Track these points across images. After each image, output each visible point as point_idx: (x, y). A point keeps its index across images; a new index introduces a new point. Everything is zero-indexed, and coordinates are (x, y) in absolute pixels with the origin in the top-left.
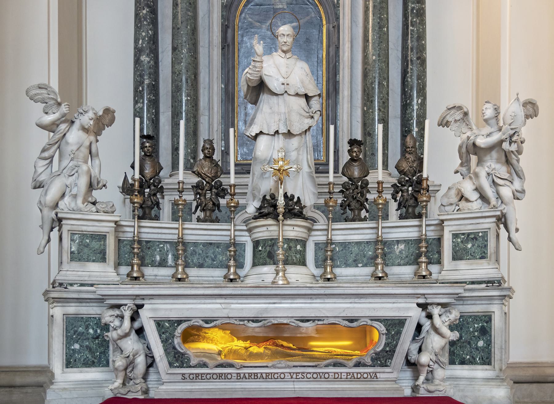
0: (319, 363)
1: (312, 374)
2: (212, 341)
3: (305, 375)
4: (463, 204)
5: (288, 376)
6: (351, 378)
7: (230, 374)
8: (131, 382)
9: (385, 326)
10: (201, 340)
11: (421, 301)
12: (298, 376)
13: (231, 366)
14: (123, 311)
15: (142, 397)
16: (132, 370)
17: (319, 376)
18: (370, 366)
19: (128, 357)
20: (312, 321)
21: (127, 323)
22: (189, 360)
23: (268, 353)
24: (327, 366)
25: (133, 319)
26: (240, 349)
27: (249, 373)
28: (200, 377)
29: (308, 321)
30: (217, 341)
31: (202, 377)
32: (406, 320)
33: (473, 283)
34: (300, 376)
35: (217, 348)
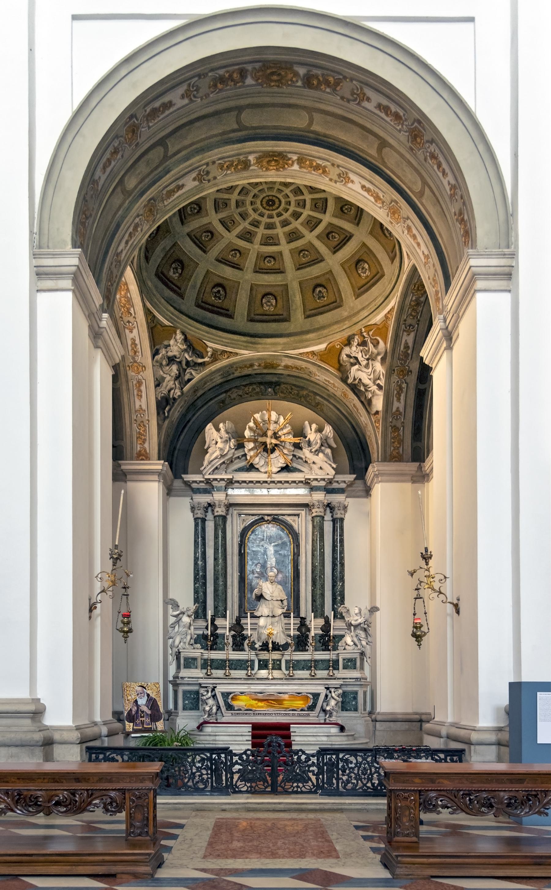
4: (347, 647)
11: (327, 686)
13: (251, 710)
21: (210, 694)
25: (212, 692)
33: (350, 679)
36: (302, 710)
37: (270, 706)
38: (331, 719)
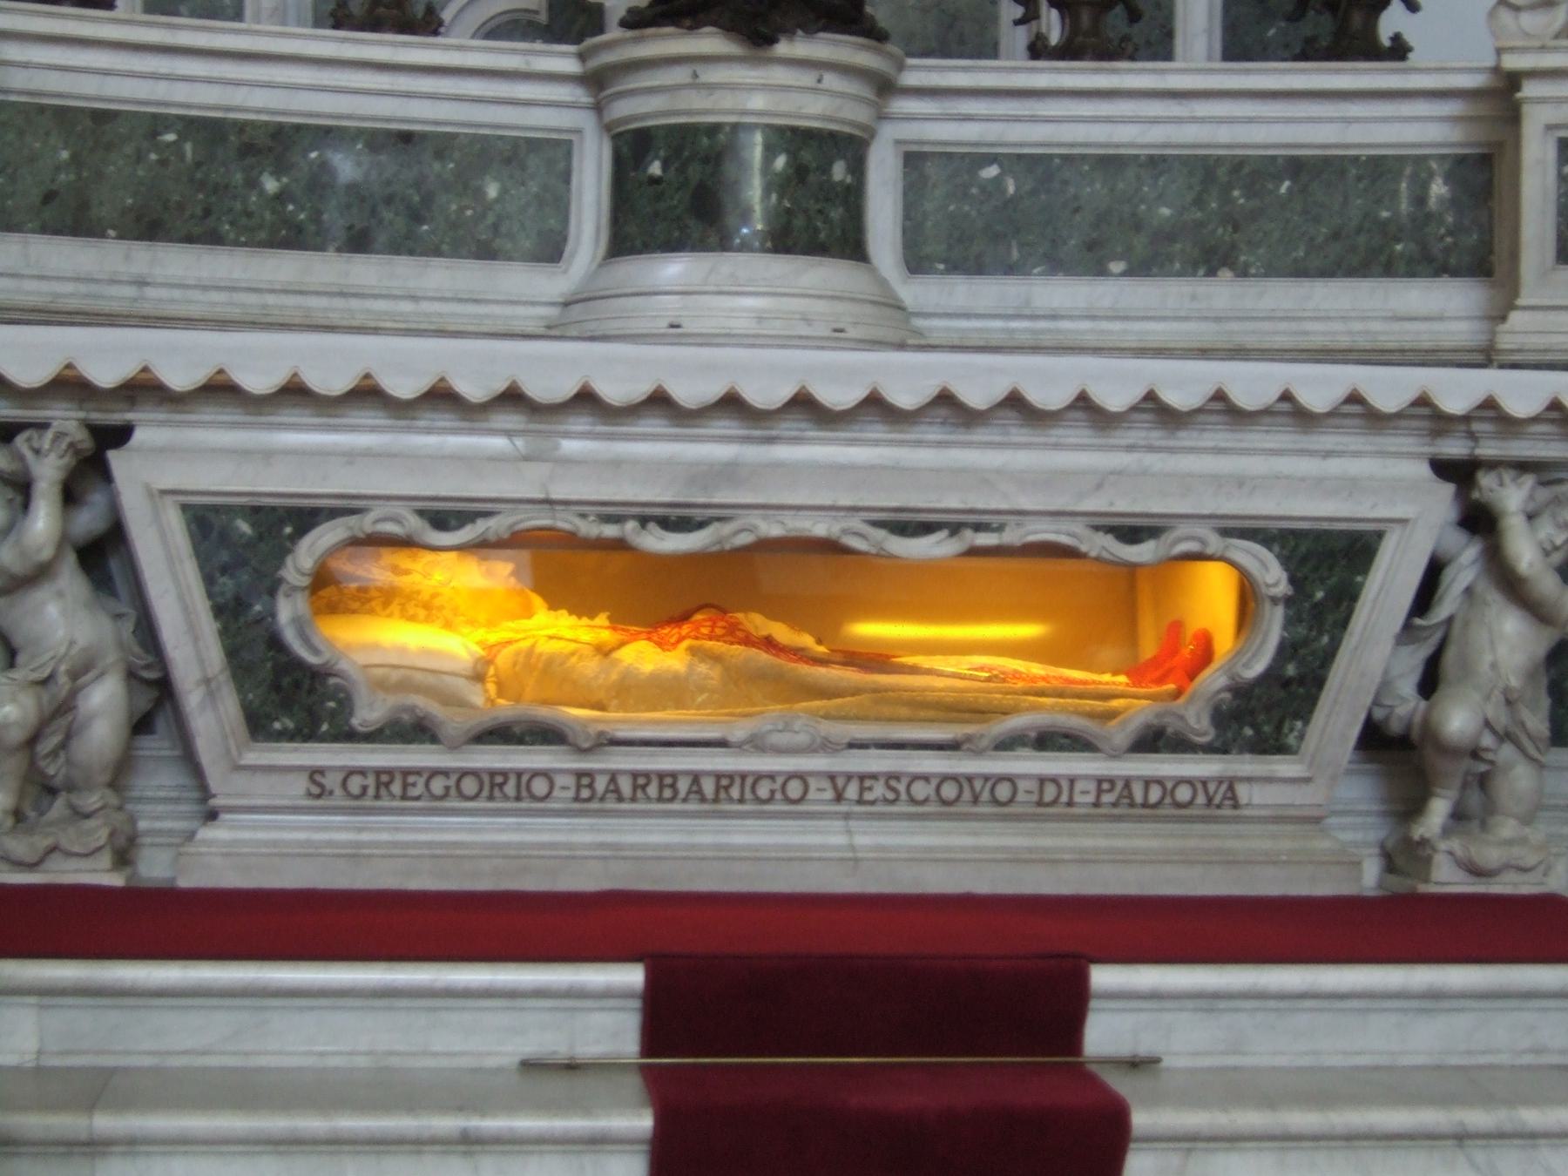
0: (970, 729)
1: (934, 782)
2: (427, 609)
3: (902, 787)
5: (821, 793)
6: (1115, 805)
7: (546, 774)
8: (58, 807)
9: (1285, 561)
10: (373, 603)
11: (1454, 448)
12: (870, 789)
13: (549, 735)
14: (29, 455)
15: (116, 880)
16: (63, 745)
17: (967, 795)
18: (1209, 749)
19: (45, 683)
20: (943, 534)
21: (43, 522)
22: (346, 703)
23: (707, 677)
24: (1007, 744)
25: (70, 496)
26: (573, 654)
27: (635, 775)
28: (396, 788)
29: (927, 528)
30: (456, 612)
31: (405, 786)
32: (1380, 535)
34: (879, 790)
35: (467, 648)
36: (1152, 741)
37: (758, 677)
38: (1490, 855)
